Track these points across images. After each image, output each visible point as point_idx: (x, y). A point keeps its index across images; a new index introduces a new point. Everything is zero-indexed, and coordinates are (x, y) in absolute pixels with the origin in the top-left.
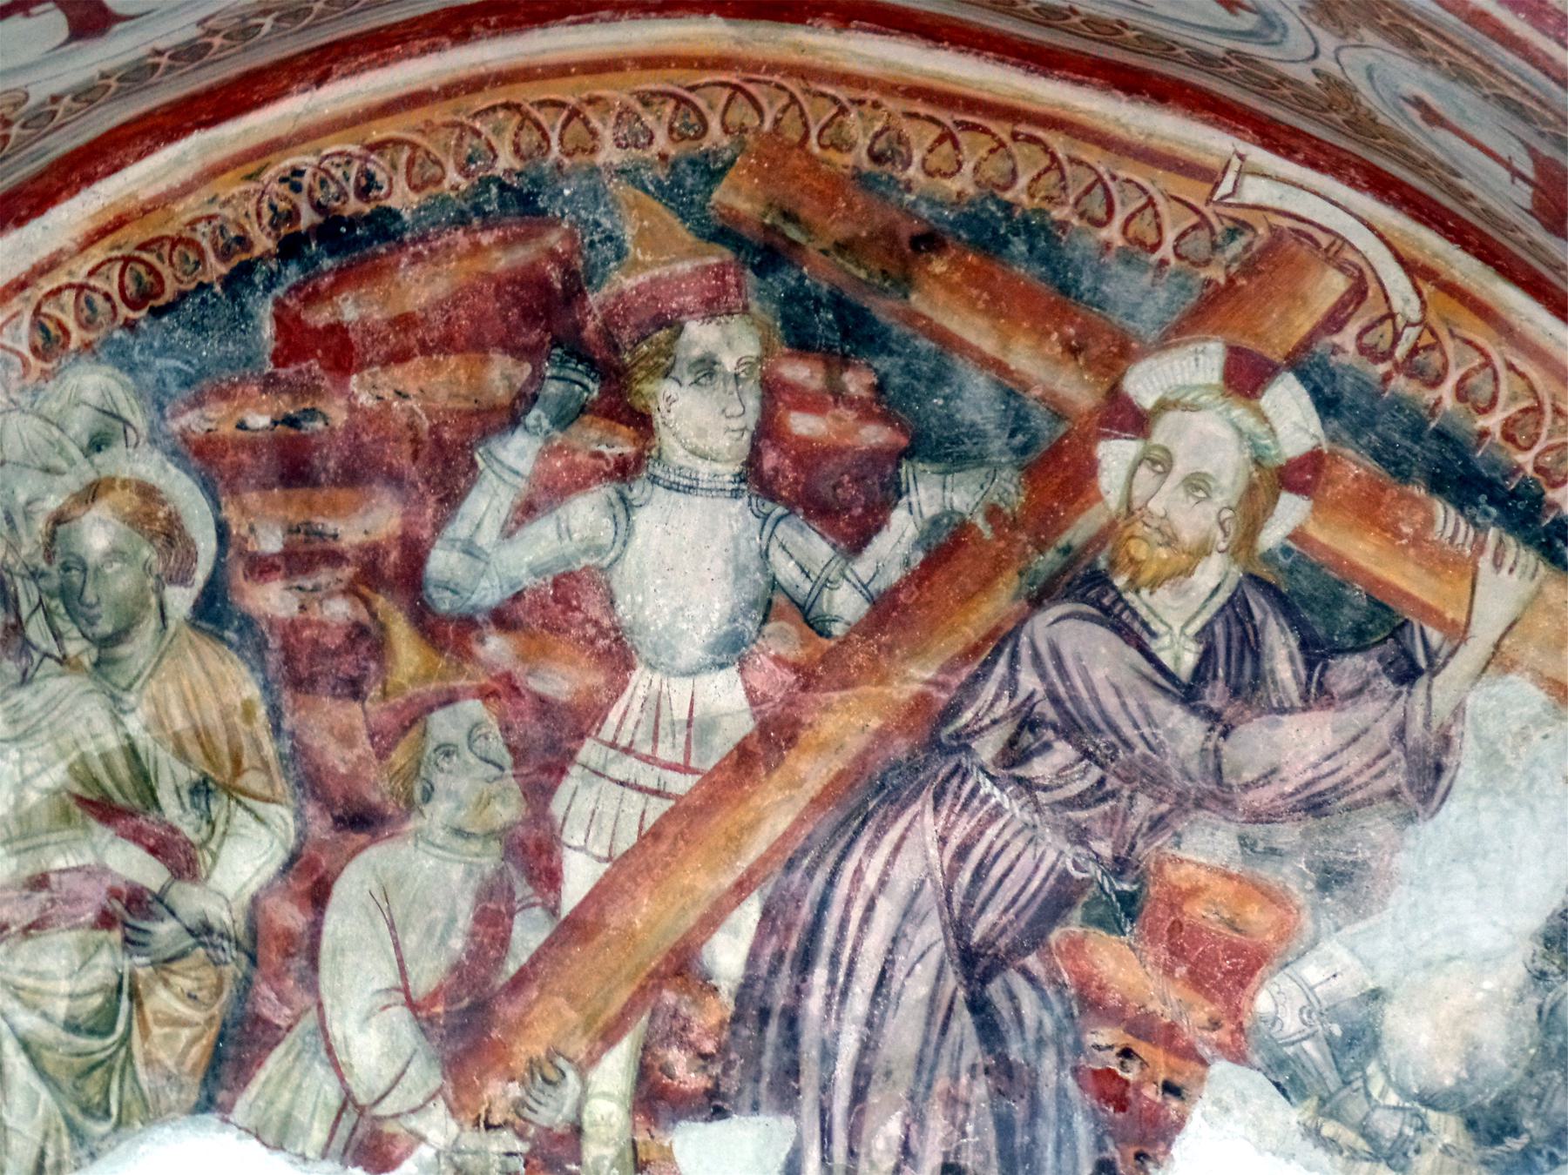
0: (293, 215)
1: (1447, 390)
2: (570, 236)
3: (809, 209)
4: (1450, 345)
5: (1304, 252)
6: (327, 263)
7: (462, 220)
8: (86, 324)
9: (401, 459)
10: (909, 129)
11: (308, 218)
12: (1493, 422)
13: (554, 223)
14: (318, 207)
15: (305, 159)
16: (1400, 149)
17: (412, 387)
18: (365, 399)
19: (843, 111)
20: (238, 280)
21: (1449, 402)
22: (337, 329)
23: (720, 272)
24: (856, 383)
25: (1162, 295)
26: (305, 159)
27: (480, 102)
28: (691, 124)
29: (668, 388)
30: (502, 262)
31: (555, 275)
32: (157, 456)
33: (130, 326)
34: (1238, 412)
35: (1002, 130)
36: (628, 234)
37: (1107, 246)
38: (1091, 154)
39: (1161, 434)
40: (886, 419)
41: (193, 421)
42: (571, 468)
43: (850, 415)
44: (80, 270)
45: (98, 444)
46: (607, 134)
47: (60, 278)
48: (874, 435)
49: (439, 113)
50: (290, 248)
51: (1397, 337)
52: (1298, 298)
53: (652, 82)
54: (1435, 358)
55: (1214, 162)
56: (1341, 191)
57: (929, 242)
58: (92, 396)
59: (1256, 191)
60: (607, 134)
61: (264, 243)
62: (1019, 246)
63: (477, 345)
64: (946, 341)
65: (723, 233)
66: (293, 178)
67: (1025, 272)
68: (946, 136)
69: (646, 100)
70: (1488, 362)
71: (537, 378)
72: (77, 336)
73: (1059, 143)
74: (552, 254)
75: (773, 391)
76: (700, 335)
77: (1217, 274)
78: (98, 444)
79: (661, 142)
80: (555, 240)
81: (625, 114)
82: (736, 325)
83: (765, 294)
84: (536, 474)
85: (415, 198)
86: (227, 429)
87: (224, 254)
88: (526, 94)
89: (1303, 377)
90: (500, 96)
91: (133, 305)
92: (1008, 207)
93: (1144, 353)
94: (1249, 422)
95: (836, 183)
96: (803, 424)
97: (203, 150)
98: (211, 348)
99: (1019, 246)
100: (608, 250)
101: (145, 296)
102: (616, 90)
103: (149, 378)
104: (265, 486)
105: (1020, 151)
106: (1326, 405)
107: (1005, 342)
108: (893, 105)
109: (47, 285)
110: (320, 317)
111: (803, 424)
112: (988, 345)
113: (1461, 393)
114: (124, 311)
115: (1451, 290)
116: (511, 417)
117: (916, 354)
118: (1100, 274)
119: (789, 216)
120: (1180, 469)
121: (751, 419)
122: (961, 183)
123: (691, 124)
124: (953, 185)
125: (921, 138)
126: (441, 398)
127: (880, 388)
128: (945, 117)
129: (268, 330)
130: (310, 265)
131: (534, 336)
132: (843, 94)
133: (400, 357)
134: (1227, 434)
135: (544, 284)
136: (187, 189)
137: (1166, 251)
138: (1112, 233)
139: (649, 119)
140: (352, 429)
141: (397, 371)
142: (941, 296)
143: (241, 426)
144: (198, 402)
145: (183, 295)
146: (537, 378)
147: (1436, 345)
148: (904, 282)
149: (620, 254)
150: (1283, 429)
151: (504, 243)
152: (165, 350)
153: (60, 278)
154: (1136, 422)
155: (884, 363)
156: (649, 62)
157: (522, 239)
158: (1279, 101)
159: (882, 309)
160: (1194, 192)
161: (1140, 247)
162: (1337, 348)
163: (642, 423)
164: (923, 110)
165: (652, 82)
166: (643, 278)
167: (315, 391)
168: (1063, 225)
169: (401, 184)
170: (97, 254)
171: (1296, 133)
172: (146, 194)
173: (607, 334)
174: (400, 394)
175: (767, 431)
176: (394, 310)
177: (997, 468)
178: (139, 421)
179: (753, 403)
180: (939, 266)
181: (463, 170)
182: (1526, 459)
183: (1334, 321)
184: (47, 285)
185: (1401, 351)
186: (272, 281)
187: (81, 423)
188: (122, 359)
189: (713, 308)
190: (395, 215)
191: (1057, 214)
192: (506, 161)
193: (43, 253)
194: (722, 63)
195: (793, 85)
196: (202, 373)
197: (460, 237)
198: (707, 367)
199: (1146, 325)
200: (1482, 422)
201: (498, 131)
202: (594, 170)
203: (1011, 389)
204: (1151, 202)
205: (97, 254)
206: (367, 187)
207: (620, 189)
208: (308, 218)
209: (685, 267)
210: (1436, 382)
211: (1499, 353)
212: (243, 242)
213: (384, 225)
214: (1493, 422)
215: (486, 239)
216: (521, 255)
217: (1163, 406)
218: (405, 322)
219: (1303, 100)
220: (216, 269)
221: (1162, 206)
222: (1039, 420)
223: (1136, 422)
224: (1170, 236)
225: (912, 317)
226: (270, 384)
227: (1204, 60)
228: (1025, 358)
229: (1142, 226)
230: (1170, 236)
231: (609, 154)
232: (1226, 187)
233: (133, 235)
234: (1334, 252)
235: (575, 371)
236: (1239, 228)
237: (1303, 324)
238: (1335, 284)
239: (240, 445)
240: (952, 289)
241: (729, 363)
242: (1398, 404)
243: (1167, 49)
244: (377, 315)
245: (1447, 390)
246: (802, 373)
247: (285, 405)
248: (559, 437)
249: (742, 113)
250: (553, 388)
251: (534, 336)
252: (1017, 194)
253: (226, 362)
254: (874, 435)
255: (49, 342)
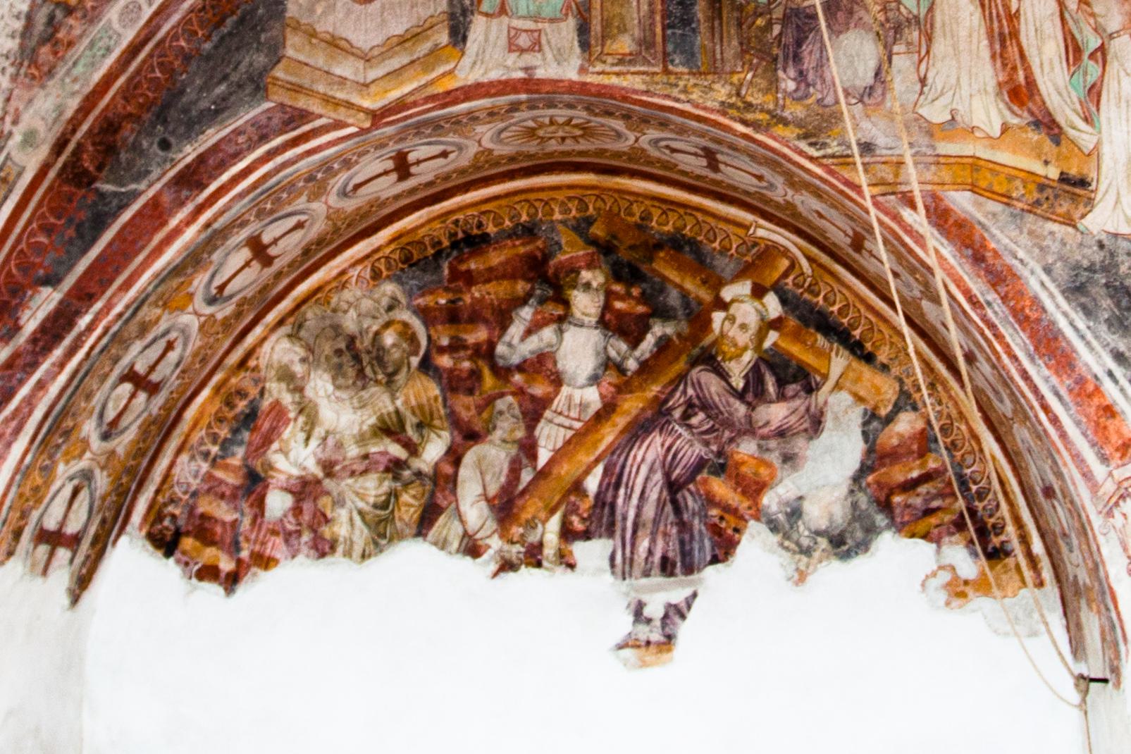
0: (456, 234)
1: (820, 298)
2: (544, 242)
3: (620, 235)
4: (821, 284)
5: (775, 252)
6: (466, 250)
7: (510, 237)
8: (388, 269)
9: (488, 314)
10: (653, 210)
11: (460, 235)
12: (835, 308)
13: (540, 238)
14: (464, 232)
15: (460, 216)
16: (809, 223)
17: (492, 291)
18: (477, 295)
19: (632, 204)
20: (438, 255)
21: (821, 302)
22: (469, 272)
23: (593, 253)
24: (635, 292)
25: (732, 266)
26: (460, 216)
27: (517, 198)
28: (583, 206)
29: (575, 292)
30: (522, 250)
31: (539, 254)
32: (409, 313)
33: (402, 270)
34: (756, 304)
35: (681, 211)
36: (563, 241)
37: (714, 249)
38: (709, 220)
39: (732, 310)
40: (645, 304)
41: (421, 301)
42: (544, 318)
43: (633, 302)
44: (387, 251)
45: (390, 308)
46: (557, 210)
47: (380, 254)
48: (641, 309)
49: (503, 202)
50: (455, 245)
51: (805, 281)
52: (774, 268)
53: (571, 193)
54: (816, 288)
55: (747, 223)
56: (787, 234)
57: (659, 246)
58: (389, 293)
59: (761, 233)
60: (557, 210)
61: (446, 243)
62: (687, 249)
63: (513, 277)
64: (665, 279)
65: (593, 242)
66: (456, 222)
67: (689, 257)
68: (664, 212)
69: (570, 199)
70: (833, 290)
71: (533, 289)
72: (385, 273)
73: (700, 216)
74: (538, 248)
75: (609, 295)
76: (586, 275)
77: (749, 258)
78: (390, 308)
79: (574, 212)
80: (539, 243)
81: (563, 204)
82: (597, 272)
83: (607, 263)
84: (532, 321)
85: (495, 230)
86: (432, 304)
87: (433, 246)
88: (532, 196)
89: (776, 293)
90: (523, 197)
91: (403, 263)
92: (684, 236)
93: (726, 284)
94: (760, 307)
95: (629, 226)
96: (619, 305)
97: (430, 212)
98: (428, 278)
99: (687, 249)
100: (556, 247)
101: (407, 260)
102: (560, 196)
103: (408, 287)
104: (443, 323)
105: (686, 218)
106: (784, 301)
107: (683, 280)
108: (648, 202)
109: (376, 256)
110: (463, 267)
111: (619, 305)
112: (678, 280)
113: (825, 298)
114: (400, 265)
115: (821, 266)
116: (523, 301)
117: (654, 283)
118: (713, 258)
119: (614, 237)
120: (738, 322)
121: (602, 303)
122: (668, 228)
123: (583, 206)
124: (666, 228)
125: (656, 213)
126: (501, 295)
127: (643, 293)
128: (664, 207)
129: (446, 272)
130: (460, 250)
131: (532, 275)
132: (632, 198)
133: (488, 281)
134: (753, 311)
135: (535, 258)
136: (422, 225)
137: (733, 251)
138: (716, 245)
139: (570, 205)
140: (472, 305)
141: (488, 286)
142: (662, 263)
143: (437, 303)
144: (423, 295)
145: (419, 260)
146: (533, 289)
147: (816, 284)
148: (651, 259)
149: (560, 248)
150: (770, 309)
151: (523, 244)
152: (413, 278)
153: (380, 254)
154: (723, 306)
155: (644, 285)
156: (571, 187)
157: (528, 243)
158: (771, 206)
159: (644, 268)
160: (741, 232)
161: (724, 250)
162: (786, 284)
163: (566, 304)
164: (657, 204)
165: (571, 193)
166: (567, 256)
167: (461, 291)
168: (701, 242)
169: (491, 225)
170: (393, 246)
171: (772, 215)
172: (409, 227)
173: (556, 274)
174: (489, 293)
175: (607, 307)
176: (487, 265)
177: (680, 321)
178: (404, 300)
179: (602, 298)
180: (662, 254)
181: (511, 220)
182: (845, 321)
183: (786, 275)
184: (376, 256)
185: (807, 285)
186: (448, 255)
187: (385, 302)
188: (399, 280)
189: (590, 266)
190: (488, 235)
191: (699, 238)
192: (524, 218)
193: (376, 245)
194: (593, 187)
195: (616, 195)
196: (425, 286)
197: (509, 242)
198: (587, 286)
199: (727, 274)
200: (831, 309)
201: (522, 207)
202: (552, 221)
203: (684, 295)
204: (728, 236)
205: (393, 246)
206: (480, 225)
207: (560, 227)
208: (460, 235)
209: (581, 253)
210: (817, 295)
211: (836, 286)
212: (440, 243)
213: (485, 238)
214: (835, 308)
215: (517, 243)
216: (529, 248)
217: (733, 301)
218: (491, 269)
219: (778, 206)
220: (431, 251)
221: (732, 237)
222: (693, 304)
223: (723, 306)
224: (734, 246)
225: (654, 270)
226: (447, 289)
227: (747, 193)
228: (689, 285)
229: (726, 242)
230: (734, 246)
231: (557, 216)
232: (751, 231)
233: (404, 240)
234: (785, 252)
235: (545, 286)
236: (755, 244)
237: (776, 275)
238: (785, 263)
239: (435, 310)
240: (666, 261)
241: (595, 284)
242: (805, 301)
243: (735, 189)
244: (482, 267)
245: (820, 298)
246: (618, 288)
247: (451, 296)
248: (539, 308)
249: (600, 204)
250: (538, 292)
251: (532, 275)
252: (687, 231)
253: (432, 282)
254: (641, 309)
255: (376, 275)
